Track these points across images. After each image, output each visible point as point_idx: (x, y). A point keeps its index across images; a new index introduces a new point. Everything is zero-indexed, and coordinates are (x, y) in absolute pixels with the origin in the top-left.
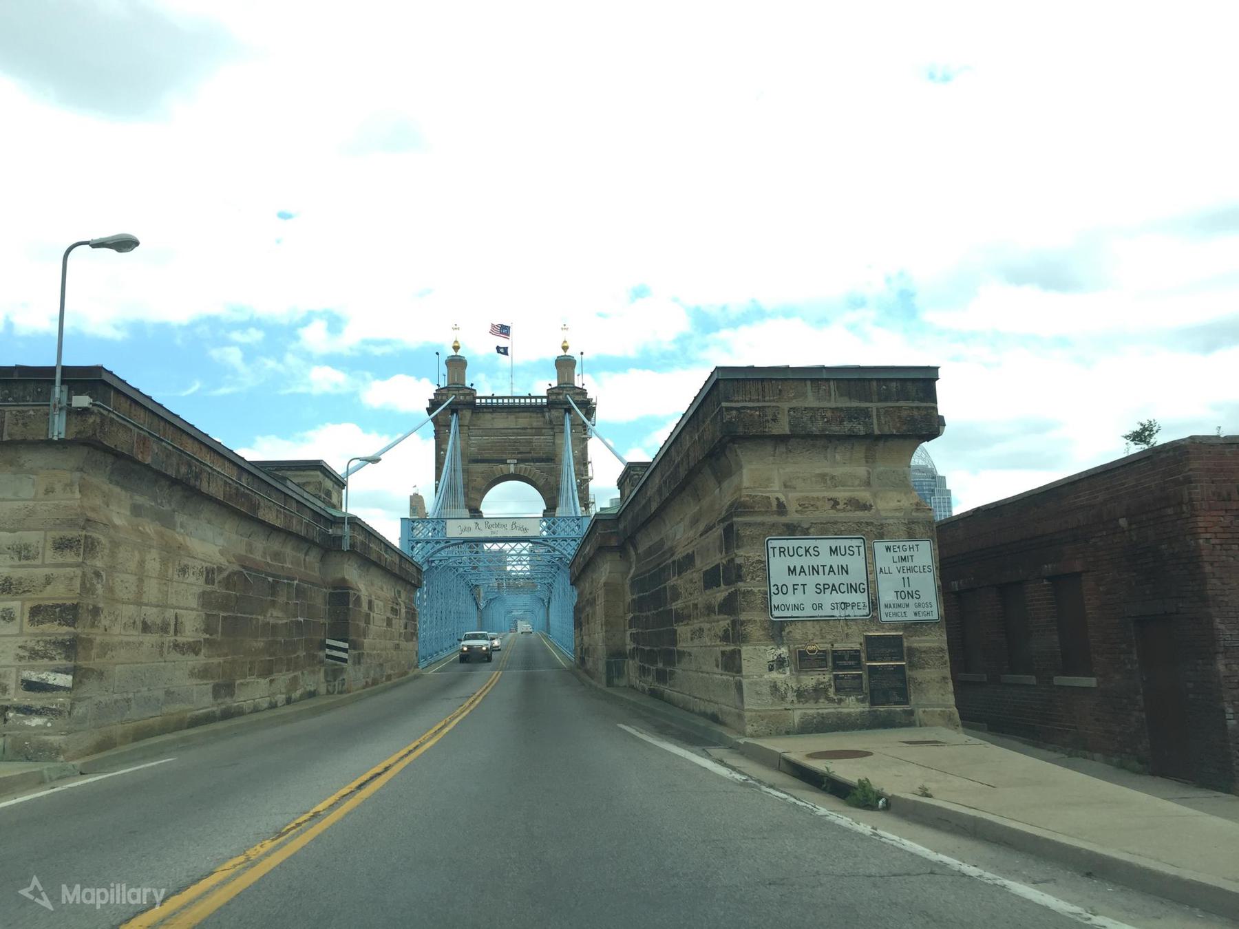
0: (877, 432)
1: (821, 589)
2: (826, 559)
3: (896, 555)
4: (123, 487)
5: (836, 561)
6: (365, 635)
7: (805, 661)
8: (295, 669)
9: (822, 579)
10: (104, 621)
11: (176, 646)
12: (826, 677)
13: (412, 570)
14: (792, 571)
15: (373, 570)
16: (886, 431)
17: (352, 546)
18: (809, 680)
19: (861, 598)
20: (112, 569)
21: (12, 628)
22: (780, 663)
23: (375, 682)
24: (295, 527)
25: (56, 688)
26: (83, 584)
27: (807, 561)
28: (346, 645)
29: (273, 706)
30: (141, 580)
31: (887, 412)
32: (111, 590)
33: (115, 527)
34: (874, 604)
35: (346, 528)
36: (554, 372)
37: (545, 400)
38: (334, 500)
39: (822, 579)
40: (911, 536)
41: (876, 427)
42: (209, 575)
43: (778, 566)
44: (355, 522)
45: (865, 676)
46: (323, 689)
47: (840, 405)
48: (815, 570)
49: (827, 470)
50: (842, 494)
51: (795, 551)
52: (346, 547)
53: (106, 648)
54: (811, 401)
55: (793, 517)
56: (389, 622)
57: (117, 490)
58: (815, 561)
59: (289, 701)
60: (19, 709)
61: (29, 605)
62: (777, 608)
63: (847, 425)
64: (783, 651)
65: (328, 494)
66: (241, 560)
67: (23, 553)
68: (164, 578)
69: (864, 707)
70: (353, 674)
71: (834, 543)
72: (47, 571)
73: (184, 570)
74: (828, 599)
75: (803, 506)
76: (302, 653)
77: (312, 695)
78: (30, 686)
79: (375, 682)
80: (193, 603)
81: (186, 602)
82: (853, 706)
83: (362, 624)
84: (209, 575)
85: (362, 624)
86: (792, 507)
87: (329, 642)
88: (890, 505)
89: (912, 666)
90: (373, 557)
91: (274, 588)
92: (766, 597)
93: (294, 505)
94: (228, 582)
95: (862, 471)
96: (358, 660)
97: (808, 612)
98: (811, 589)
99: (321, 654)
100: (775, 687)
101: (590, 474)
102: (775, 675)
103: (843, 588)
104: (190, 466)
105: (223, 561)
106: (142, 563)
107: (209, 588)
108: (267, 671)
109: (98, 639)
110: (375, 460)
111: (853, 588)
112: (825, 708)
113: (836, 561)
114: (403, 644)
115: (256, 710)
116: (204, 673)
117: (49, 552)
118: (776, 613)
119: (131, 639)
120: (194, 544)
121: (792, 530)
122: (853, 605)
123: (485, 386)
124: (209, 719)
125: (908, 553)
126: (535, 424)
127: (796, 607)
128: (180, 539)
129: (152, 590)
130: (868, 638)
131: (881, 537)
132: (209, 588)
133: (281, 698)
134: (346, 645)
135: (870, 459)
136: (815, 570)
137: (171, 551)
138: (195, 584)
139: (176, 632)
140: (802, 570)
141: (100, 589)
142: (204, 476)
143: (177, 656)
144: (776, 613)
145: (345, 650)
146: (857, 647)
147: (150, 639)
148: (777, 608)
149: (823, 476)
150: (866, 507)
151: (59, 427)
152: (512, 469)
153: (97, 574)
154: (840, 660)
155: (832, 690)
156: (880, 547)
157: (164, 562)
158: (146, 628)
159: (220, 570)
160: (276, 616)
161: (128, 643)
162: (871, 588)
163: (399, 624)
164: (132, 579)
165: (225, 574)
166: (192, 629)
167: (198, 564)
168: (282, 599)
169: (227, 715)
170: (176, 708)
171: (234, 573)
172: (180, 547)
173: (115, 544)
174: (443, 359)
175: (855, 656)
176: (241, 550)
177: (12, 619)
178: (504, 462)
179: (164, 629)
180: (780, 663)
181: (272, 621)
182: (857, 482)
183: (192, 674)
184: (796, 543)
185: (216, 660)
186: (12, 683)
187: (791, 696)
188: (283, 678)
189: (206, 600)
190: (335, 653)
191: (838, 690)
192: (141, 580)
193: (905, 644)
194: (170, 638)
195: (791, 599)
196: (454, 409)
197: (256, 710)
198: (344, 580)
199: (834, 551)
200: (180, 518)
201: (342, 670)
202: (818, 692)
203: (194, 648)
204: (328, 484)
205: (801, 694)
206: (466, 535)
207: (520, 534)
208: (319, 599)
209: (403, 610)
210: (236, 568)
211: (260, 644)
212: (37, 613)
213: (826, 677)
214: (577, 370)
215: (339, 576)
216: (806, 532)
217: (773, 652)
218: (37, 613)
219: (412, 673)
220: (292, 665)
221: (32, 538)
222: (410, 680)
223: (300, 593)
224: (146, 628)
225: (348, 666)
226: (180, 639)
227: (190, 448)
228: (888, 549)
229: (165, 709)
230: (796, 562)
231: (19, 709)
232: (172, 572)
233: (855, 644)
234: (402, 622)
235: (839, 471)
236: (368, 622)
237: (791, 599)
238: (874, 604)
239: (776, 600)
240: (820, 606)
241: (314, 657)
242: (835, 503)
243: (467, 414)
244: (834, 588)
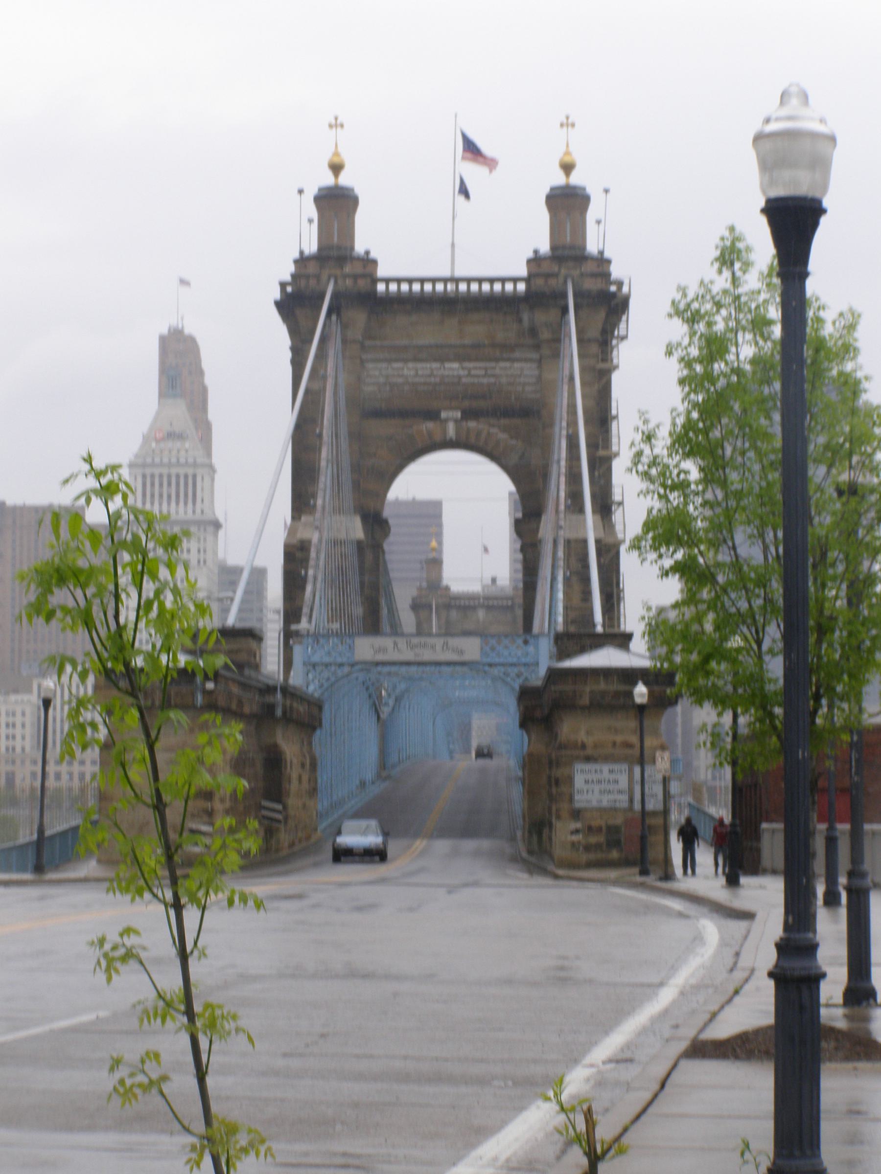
2: (606, 774)
5: (612, 777)
9: (603, 786)
19: (625, 798)
22: (577, 831)
27: (595, 777)
35: (279, 695)
36: (542, 218)
37: (521, 287)
39: (603, 786)
43: (579, 781)
48: (599, 782)
50: (619, 739)
52: (279, 712)
54: (602, 686)
55: (589, 752)
64: (579, 825)
75: (596, 746)
101: (615, 448)
111: (620, 792)
112: (600, 856)
121: (588, 759)
123: (402, 247)
126: (500, 336)
136: (599, 782)
151: (199, 699)
152: (451, 431)
174: (311, 192)
178: (432, 415)
180: (577, 831)
199: (611, 771)
202: (598, 847)
205: (588, 848)
206: (380, 657)
207: (454, 657)
214: (592, 214)
230: (589, 777)
239: (577, 797)
242: (614, 744)
243: (359, 317)
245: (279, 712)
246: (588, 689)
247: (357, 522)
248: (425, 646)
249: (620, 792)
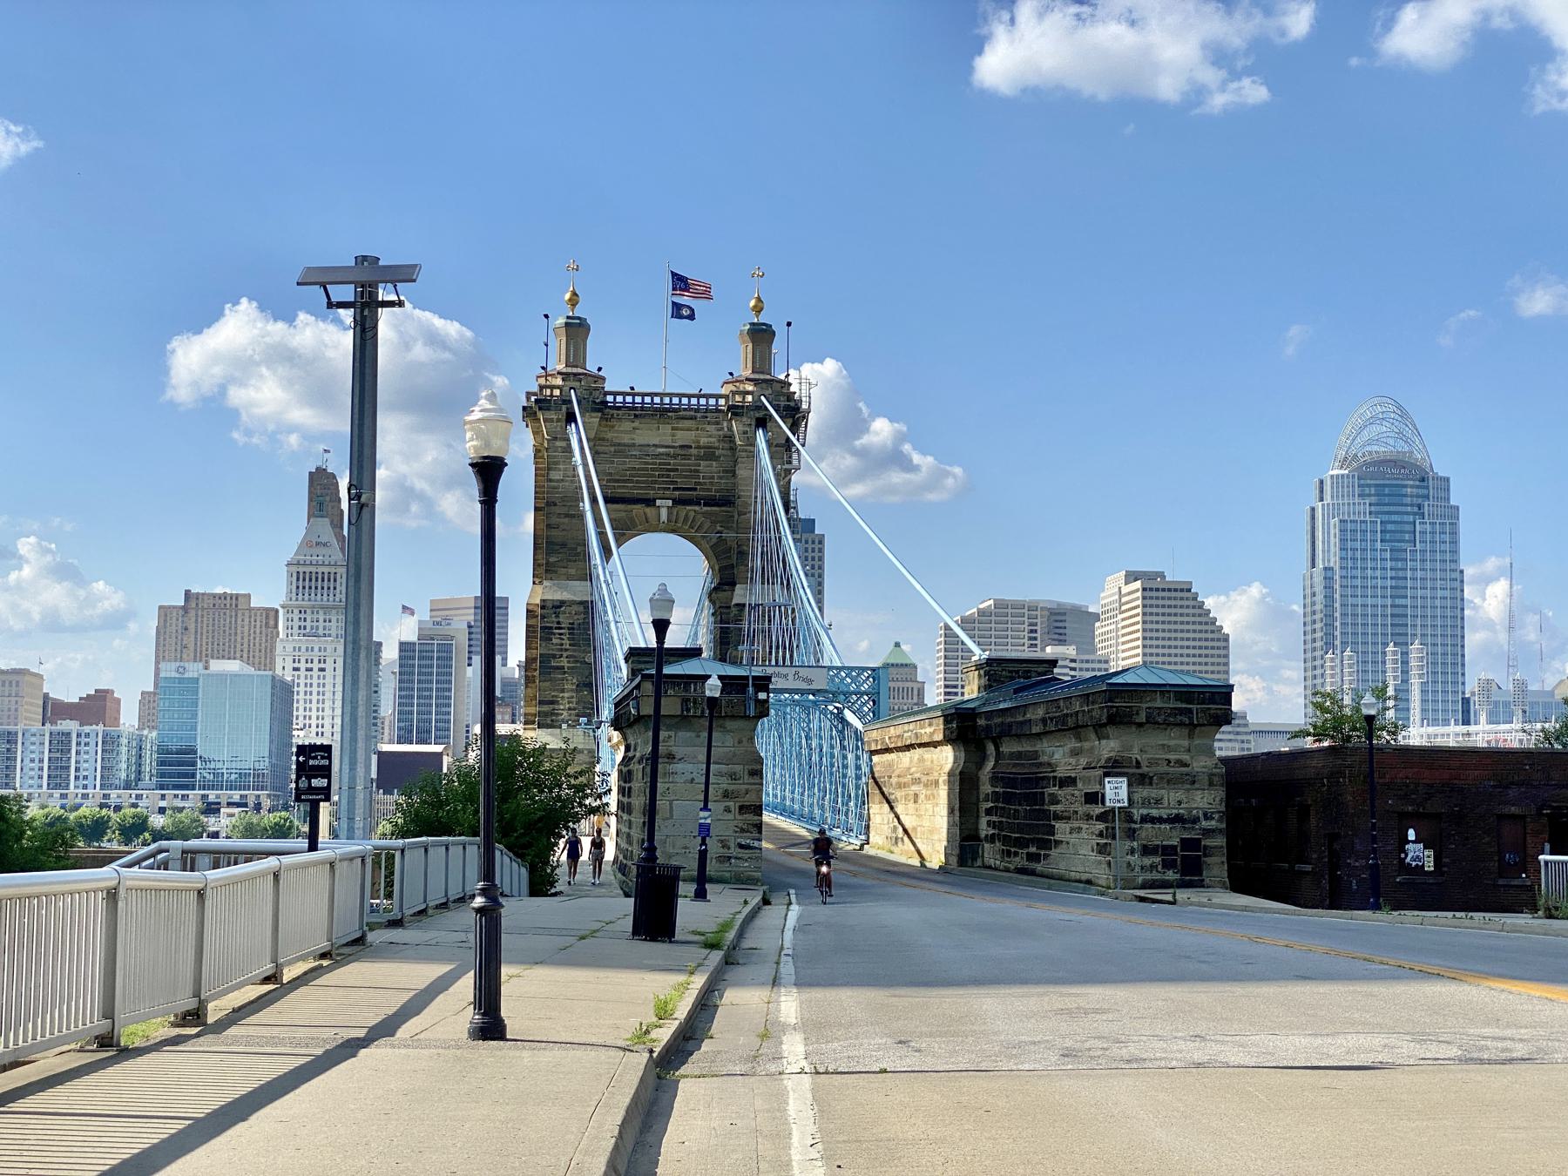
18: (1147, 861)
21: (731, 816)
31: (1203, 711)
50: (1172, 757)
54: (1159, 704)
67: (733, 776)
69: (1177, 876)
78: (741, 846)
82: (1171, 875)
86: (1144, 764)
88: (1200, 764)
95: (1186, 743)
100: (1129, 864)
112: (1155, 876)
135: (1191, 736)
150: (1186, 765)
180: (1132, 852)
187: (1137, 869)
202: (1153, 867)
212: (743, 809)
213: (1158, 859)
217: (1128, 844)
218: (741, 808)
221: (738, 768)
235: (1172, 743)
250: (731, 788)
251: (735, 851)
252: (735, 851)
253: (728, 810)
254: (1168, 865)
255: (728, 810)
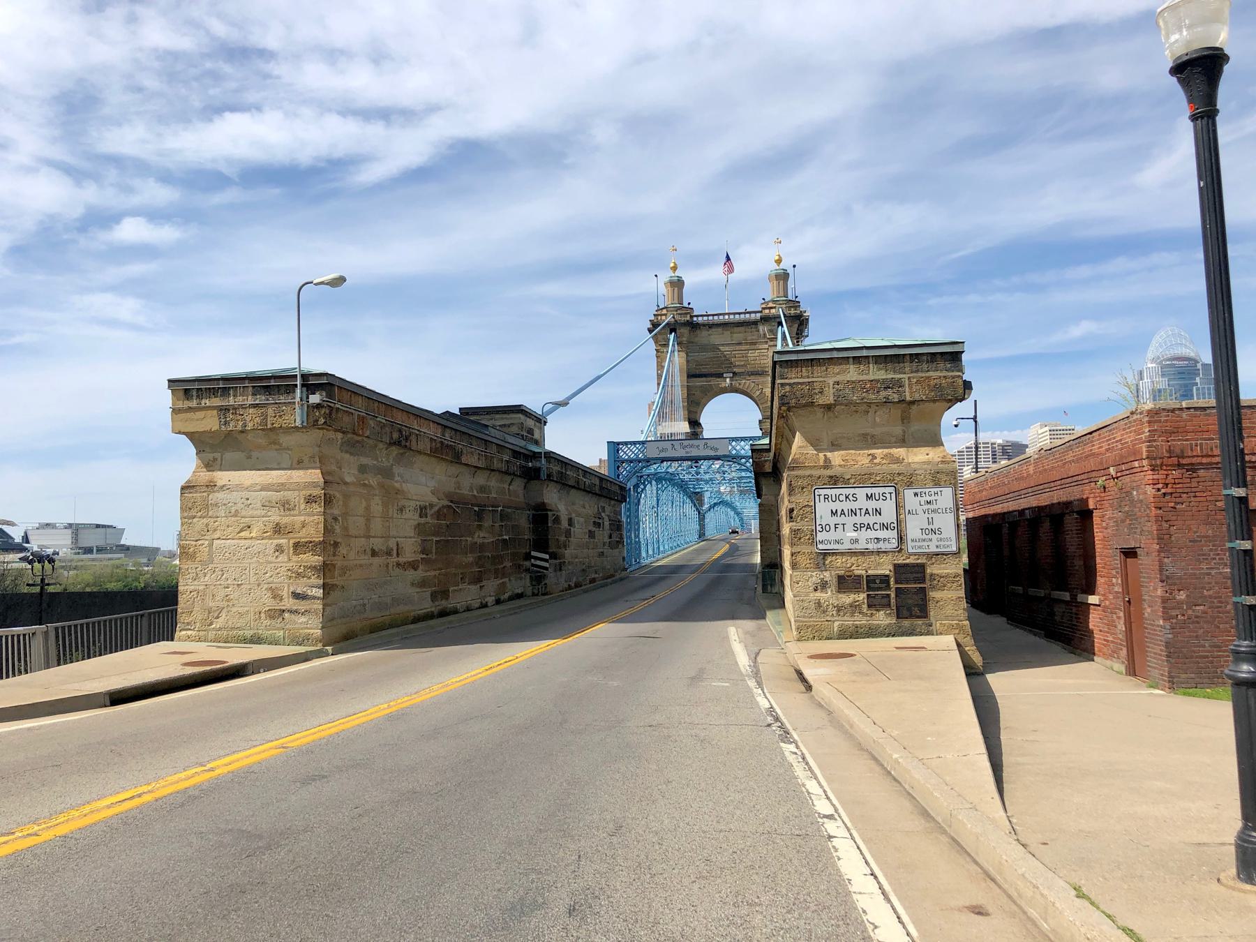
0: (908, 398)
1: (857, 528)
2: (862, 503)
3: (923, 500)
4: (351, 454)
5: (872, 505)
6: (565, 547)
7: (846, 583)
8: (504, 576)
9: (858, 519)
10: (343, 550)
11: (398, 564)
12: (862, 596)
13: (614, 488)
14: (834, 513)
15: (573, 491)
16: (917, 397)
17: (549, 476)
18: (847, 599)
19: (893, 534)
20: (345, 515)
21: (284, 558)
23: (578, 585)
24: (496, 465)
25: (315, 598)
26: (325, 527)
27: (846, 506)
28: (547, 557)
29: (484, 606)
30: (368, 520)
32: (346, 529)
33: (346, 483)
34: (901, 539)
38: (536, 436)
39: (858, 519)
40: (937, 484)
41: (907, 394)
42: (422, 511)
43: (823, 509)
44: (550, 456)
45: (893, 595)
46: (529, 591)
47: (876, 377)
48: (853, 512)
49: (869, 430)
51: (837, 497)
53: (344, 570)
56: (591, 535)
57: (347, 456)
58: (854, 506)
59: (498, 602)
60: (290, 611)
61: (292, 541)
62: (821, 542)
63: (883, 393)
64: (827, 575)
65: (530, 431)
66: (451, 498)
67: (286, 506)
68: (386, 517)
70: (554, 580)
71: (869, 491)
72: (302, 518)
73: (401, 510)
74: (865, 535)
76: (508, 564)
77: (519, 596)
78: (296, 596)
79: (578, 585)
80: (411, 532)
81: (405, 532)
82: (883, 618)
83: (563, 538)
84: (422, 511)
85: (563, 538)
87: (533, 553)
89: (933, 588)
90: (571, 483)
91: (479, 516)
92: (813, 533)
93: (494, 447)
94: (439, 515)
95: (898, 430)
96: (560, 568)
97: (846, 546)
98: (849, 526)
99: (527, 564)
100: (819, 604)
102: (818, 594)
103: (876, 527)
104: (400, 431)
105: (435, 500)
106: (368, 508)
107: (423, 520)
108: (477, 579)
109: (339, 564)
110: (564, 404)
111: (884, 527)
112: (861, 620)
113: (872, 505)
114: (607, 551)
115: (468, 609)
116: (423, 584)
117: (303, 506)
118: (820, 546)
119: (362, 562)
120: (410, 488)
121: (834, 481)
122: (885, 540)
124: (430, 616)
125: (933, 498)
127: (837, 542)
128: (397, 485)
129: (377, 526)
130: (897, 567)
131: (910, 485)
132: (423, 520)
133: (490, 600)
134: (547, 557)
136: (853, 512)
137: (392, 495)
138: (412, 517)
139: (398, 555)
140: (843, 512)
141: (337, 528)
142: (413, 438)
143: (397, 571)
144: (820, 546)
145: (546, 560)
146: (887, 572)
147: (376, 560)
148: (821, 542)
149: (865, 435)
153: (335, 519)
154: (874, 583)
155: (865, 606)
156: (909, 493)
157: (385, 505)
158: (374, 553)
159: (431, 506)
160: (481, 537)
161: (361, 566)
162: (900, 528)
163: (603, 535)
164: (361, 521)
165: (436, 508)
166: (410, 552)
167: (413, 504)
168: (487, 523)
169: (443, 614)
170: (402, 609)
171: (443, 507)
172: (398, 492)
173: (346, 497)
175: (885, 580)
176: (450, 487)
177: (283, 552)
178: (720, 376)
179: (389, 553)
180: (823, 585)
181: (479, 541)
182: (893, 439)
183: (413, 584)
184: (838, 491)
185: (433, 573)
186: (285, 593)
188: (491, 585)
189: (419, 528)
190: (538, 563)
191: (869, 606)
192: (368, 520)
193: (928, 571)
194: (394, 559)
195: (832, 536)
196: (672, 328)
197: (468, 609)
198: (543, 504)
199: (869, 497)
200: (397, 470)
201: (544, 576)
202: (854, 607)
203: (413, 566)
204: (530, 423)
205: (839, 609)
206: (663, 455)
207: (712, 453)
208: (523, 521)
209: (607, 523)
210: (446, 503)
211: (470, 558)
213: (862, 596)
215: (540, 500)
216: (846, 482)
217: (815, 577)
218: (296, 545)
219: (618, 577)
220: (499, 573)
221: (289, 495)
222: (615, 582)
223: (503, 517)
224: (374, 553)
225: (551, 574)
226: (401, 560)
227: (400, 418)
228: (916, 494)
229: (393, 611)
230: (837, 506)
231: (290, 611)
232: (393, 511)
233: (886, 569)
234: (607, 533)
235: (877, 431)
236: (568, 534)
237: (832, 536)
238: (901, 539)
239: (820, 536)
240: (857, 541)
241: (520, 566)
243: (685, 331)
244: (868, 527)
245: (543, 476)
246: (831, 381)
247: (686, 424)
248: (692, 446)
249: (884, 527)
250: (285, 520)
251: (289, 603)
252: (289, 603)
253: (279, 549)
254: (874, 604)
255: (279, 549)
